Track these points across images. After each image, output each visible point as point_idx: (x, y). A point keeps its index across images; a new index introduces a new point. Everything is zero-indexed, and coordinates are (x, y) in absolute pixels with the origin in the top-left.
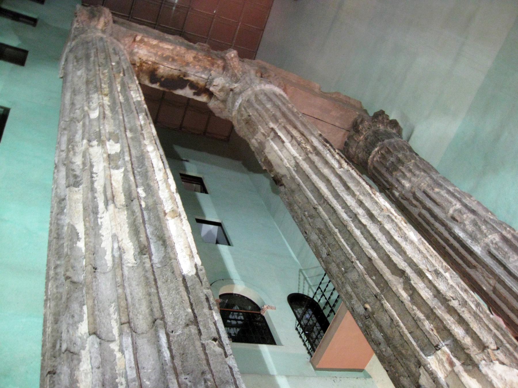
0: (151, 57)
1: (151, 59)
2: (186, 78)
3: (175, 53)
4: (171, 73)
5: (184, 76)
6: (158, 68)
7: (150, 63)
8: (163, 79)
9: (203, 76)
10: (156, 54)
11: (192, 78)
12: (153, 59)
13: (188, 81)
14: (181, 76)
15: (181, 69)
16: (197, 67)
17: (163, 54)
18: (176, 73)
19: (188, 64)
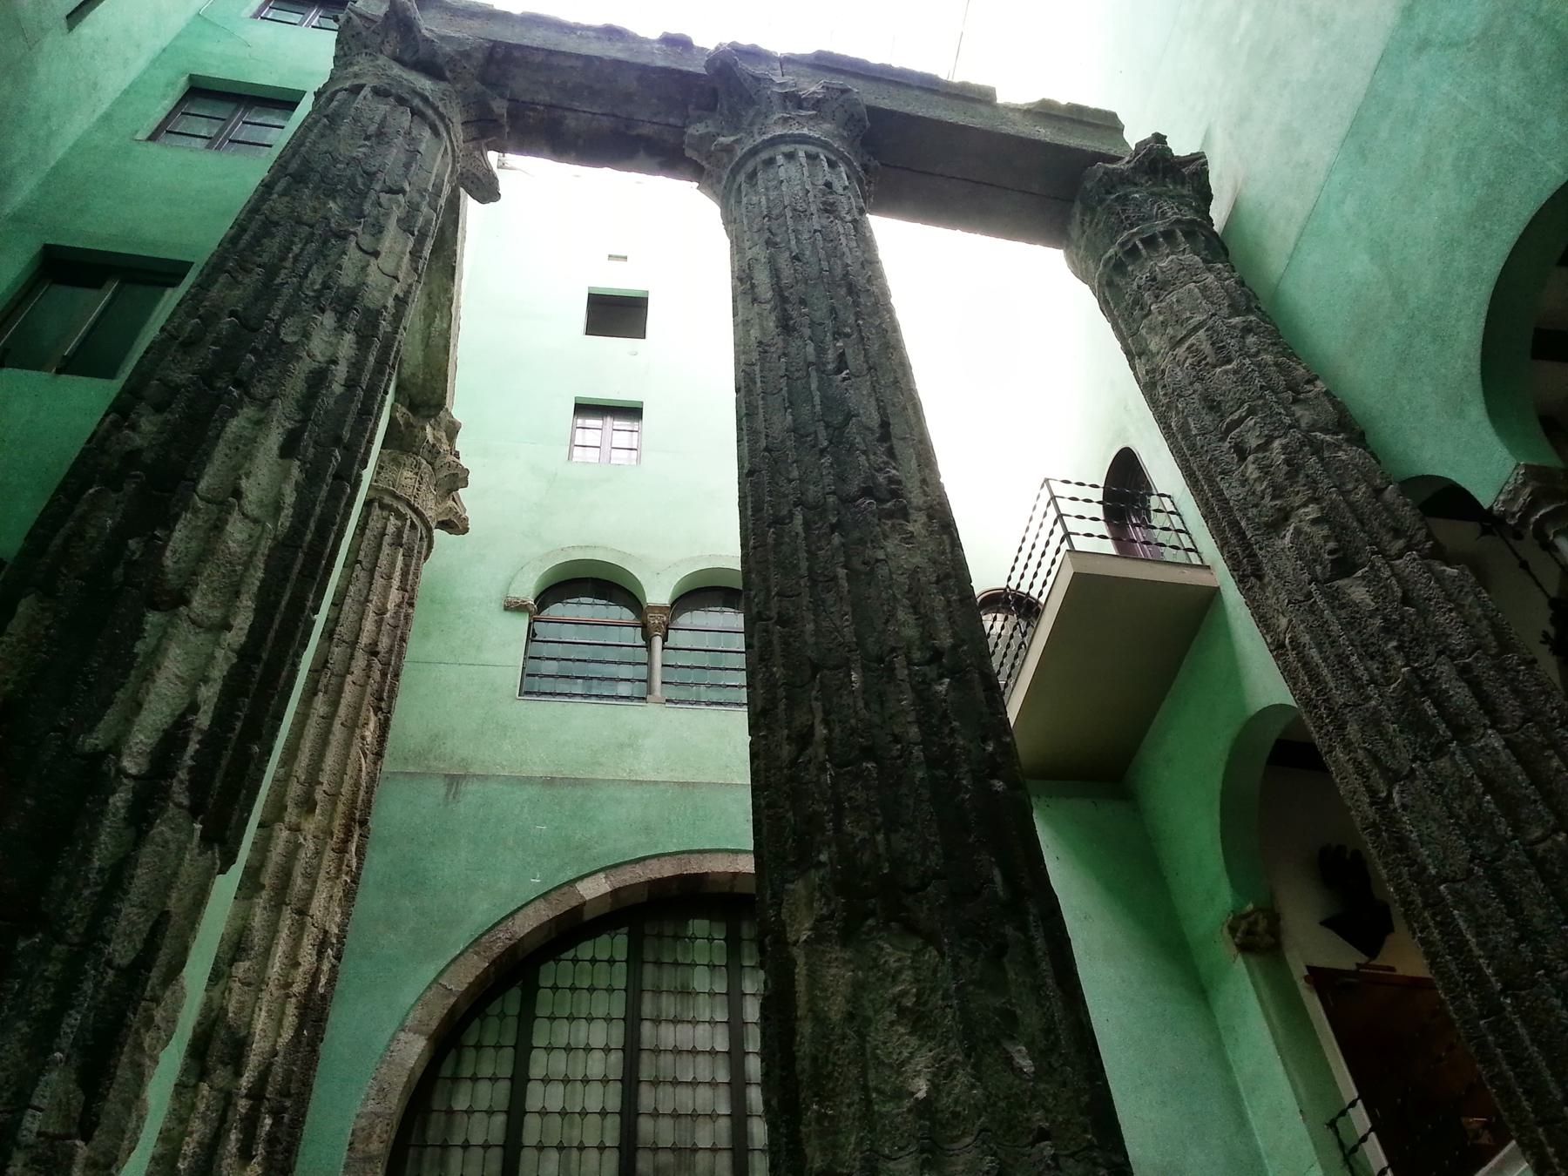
1: (541, 97)
5: (628, 127)
6: (565, 117)
9: (671, 120)
11: (646, 130)
12: (544, 97)
15: (616, 111)
18: (606, 123)
19: (628, 97)
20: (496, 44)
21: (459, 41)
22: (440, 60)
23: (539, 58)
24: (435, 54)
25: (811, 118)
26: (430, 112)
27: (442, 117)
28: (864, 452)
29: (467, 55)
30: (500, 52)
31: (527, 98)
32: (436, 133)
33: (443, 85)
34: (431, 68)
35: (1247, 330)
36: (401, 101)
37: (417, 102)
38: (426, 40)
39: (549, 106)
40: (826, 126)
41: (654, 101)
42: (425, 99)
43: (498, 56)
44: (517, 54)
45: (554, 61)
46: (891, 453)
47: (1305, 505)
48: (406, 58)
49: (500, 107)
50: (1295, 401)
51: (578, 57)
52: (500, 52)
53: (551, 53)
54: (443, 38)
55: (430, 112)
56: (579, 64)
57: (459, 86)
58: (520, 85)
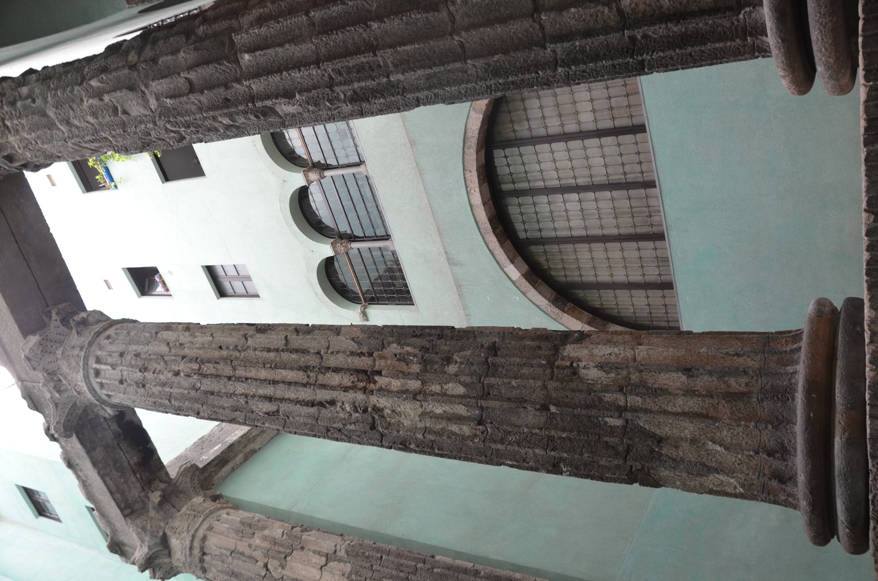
0: (133, 482)
1: (134, 480)
2: (120, 430)
3: (108, 470)
4: (129, 449)
5: (120, 435)
6: (135, 464)
7: (138, 476)
8: (141, 448)
10: (126, 482)
13: (120, 427)
14: (122, 437)
15: (116, 446)
16: (99, 435)
17: (120, 477)
18: (124, 446)
19: (106, 447)
20: (125, 516)
21: (138, 534)
22: (158, 540)
23: (118, 496)
24: (156, 544)
25: (66, 378)
26: (197, 544)
27: (193, 537)
28: (345, 425)
29: (144, 529)
30: (126, 512)
31: (138, 485)
32: (204, 539)
33: (168, 533)
34: (164, 541)
35: (68, 123)
36: (202, 561)
37: (196, 552)
38: (150, 548)
39: (135, 473)
40: (65, 369)
41: (99, 435)
42: (191, 548)
43: (129, 511)
44: (123, 505)
45: (114, 489)
46: (332, 403)
47: (221, 122)
48: (167, 552)
49: (155, 497)
50: (125, 112)
51: (105, 482)
52: (126, 512)
53: (111, 493)
54: (143, 541)
55: (197, 544)
56: (107, 479)
57: (162, 524)
58: (135, 492)
